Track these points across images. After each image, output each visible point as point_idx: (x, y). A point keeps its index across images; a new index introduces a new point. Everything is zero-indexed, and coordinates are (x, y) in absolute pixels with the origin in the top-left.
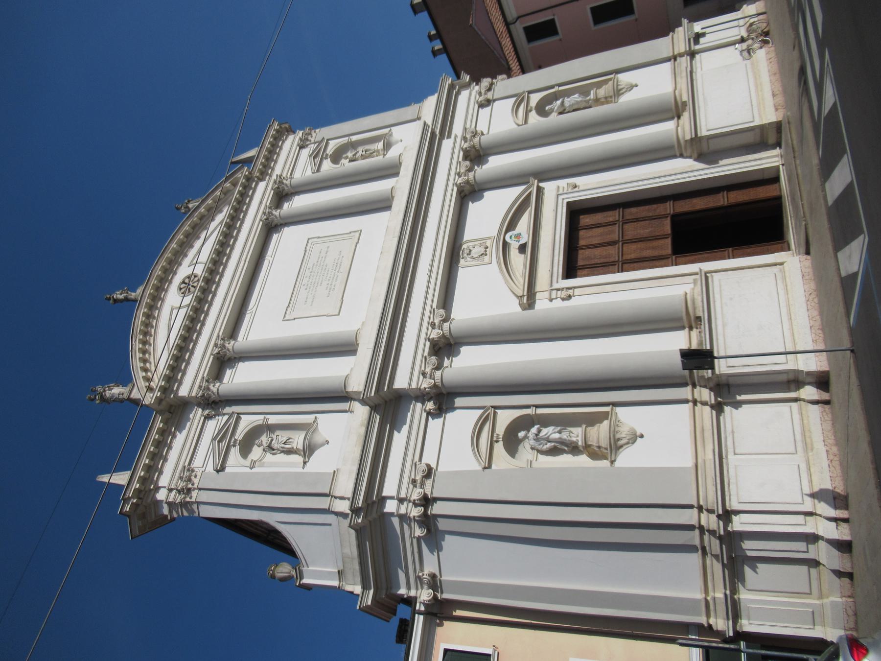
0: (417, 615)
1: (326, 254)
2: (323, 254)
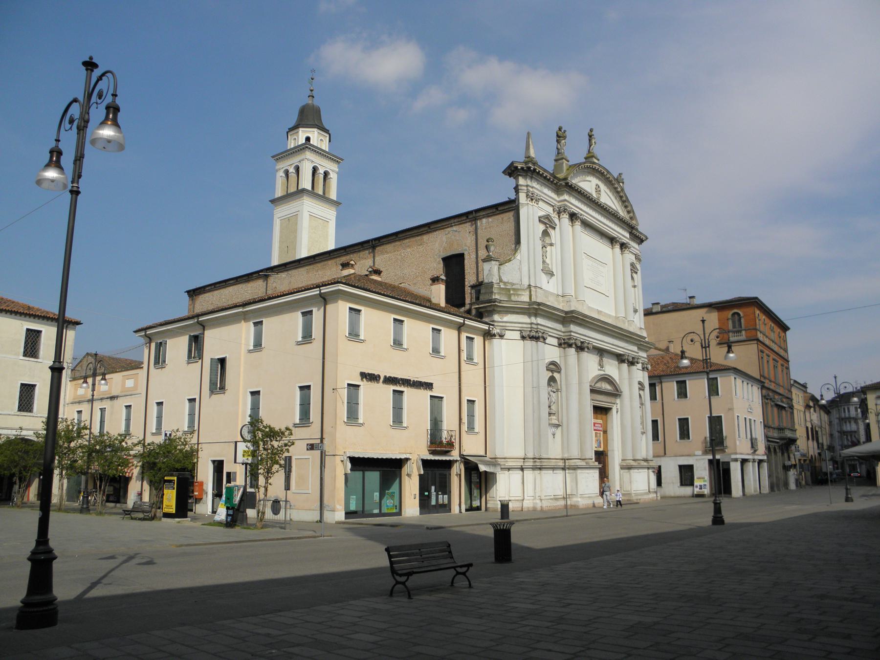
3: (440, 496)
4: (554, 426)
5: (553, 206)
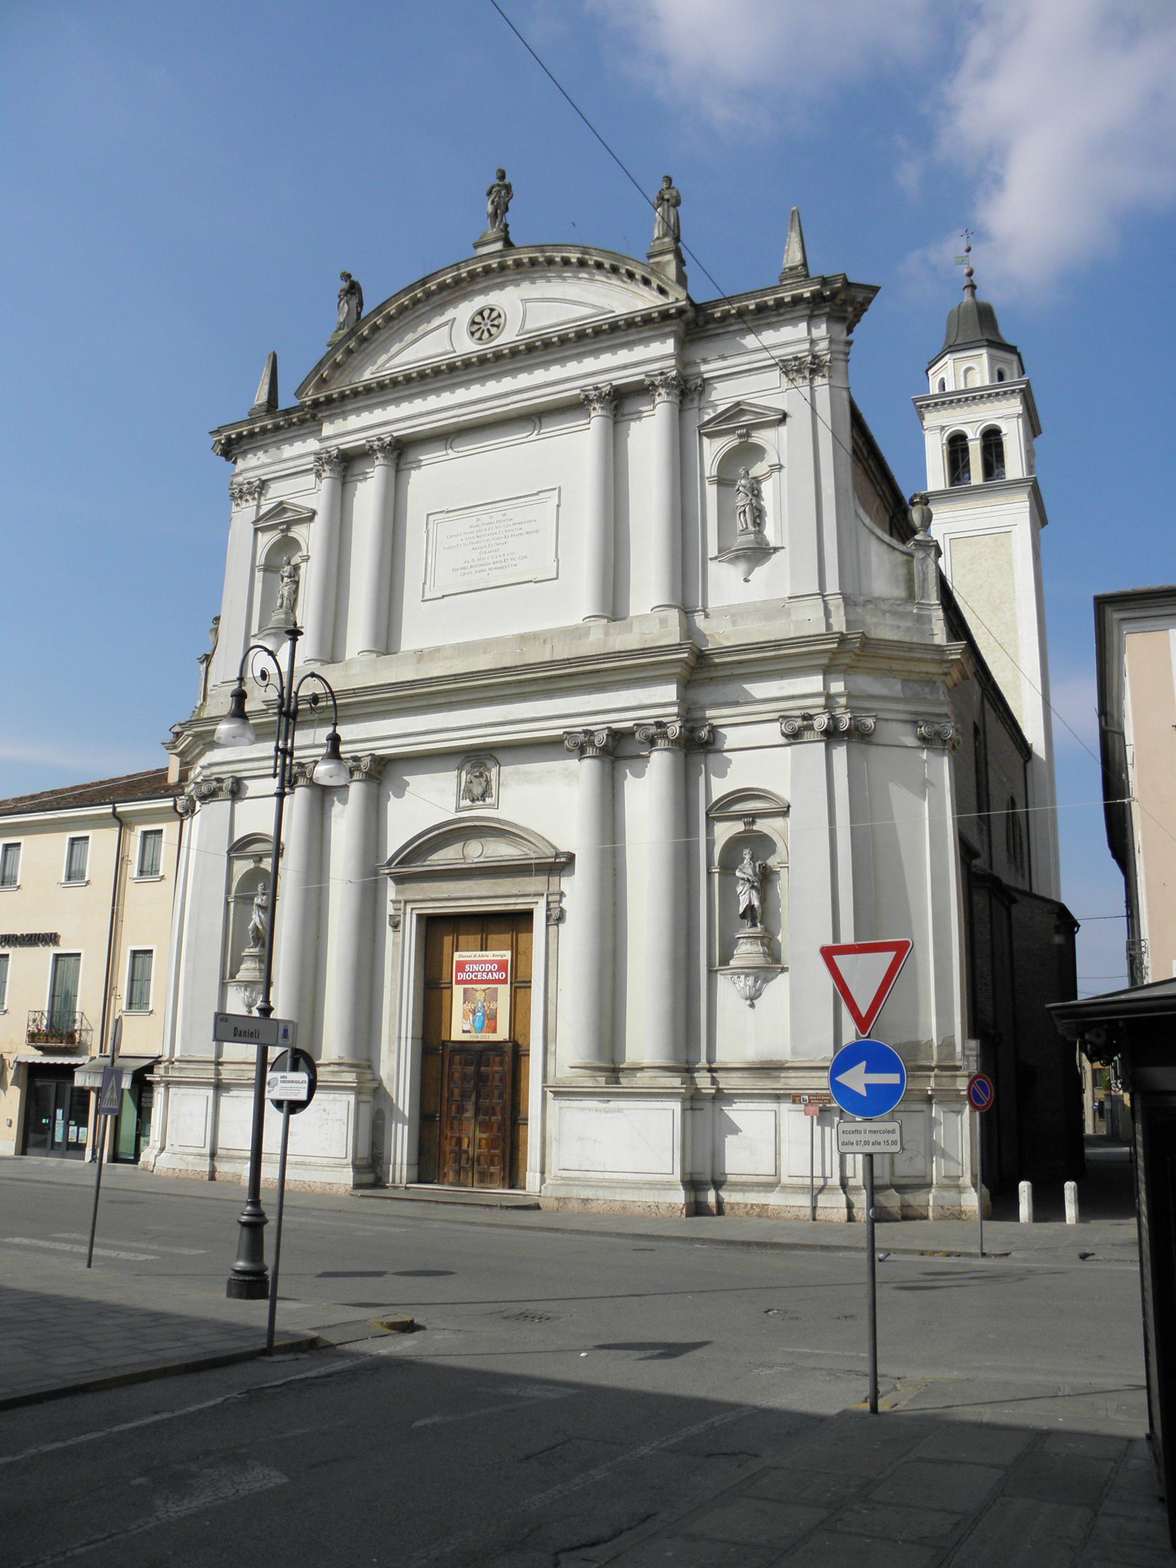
0: (172, 799)
1: (527, 533)
3: (71, 1128)
5: (311, 469)
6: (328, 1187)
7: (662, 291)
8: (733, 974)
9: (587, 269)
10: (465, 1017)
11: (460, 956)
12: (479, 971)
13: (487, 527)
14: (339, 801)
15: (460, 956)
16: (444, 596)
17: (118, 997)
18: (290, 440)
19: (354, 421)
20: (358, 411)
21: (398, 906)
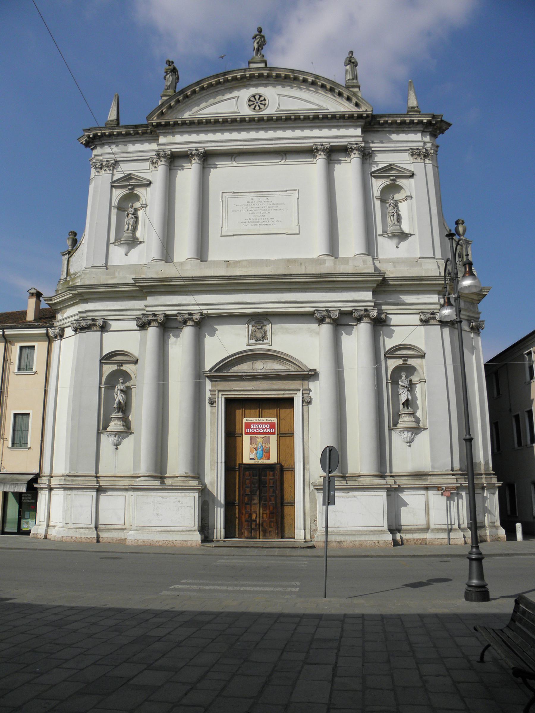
0: (45, 329)
1: (280, 209)
2: (280, 207)
4: (111, 435)
5: (148, 159)
6: (185, 543)
7: (357, 105)
8: (401, 431)
9: (314, 86)
10: (251, 451)
11: (247, 420)
12: (259, 428)
13: (258, 204)
14: (173, 336)
15: (247, 420)
16: (234, 235)
17: (5, 440)
18: (134, 142)
19: (178, 138)
20: (182, 133)
21: (214, 393)
